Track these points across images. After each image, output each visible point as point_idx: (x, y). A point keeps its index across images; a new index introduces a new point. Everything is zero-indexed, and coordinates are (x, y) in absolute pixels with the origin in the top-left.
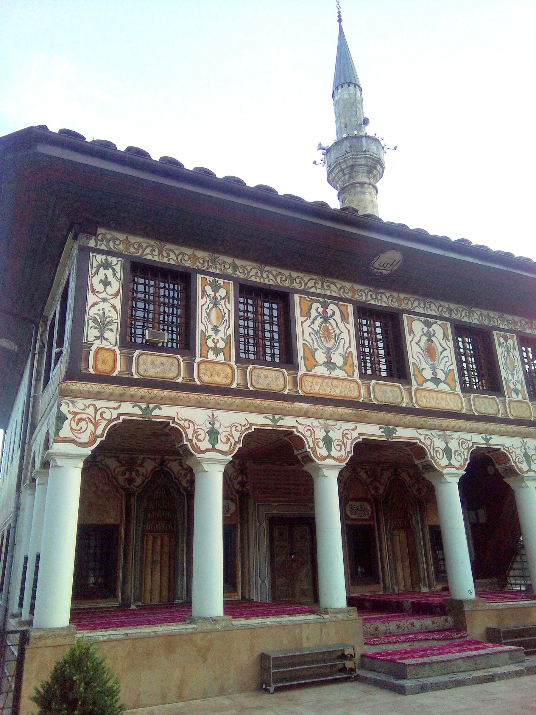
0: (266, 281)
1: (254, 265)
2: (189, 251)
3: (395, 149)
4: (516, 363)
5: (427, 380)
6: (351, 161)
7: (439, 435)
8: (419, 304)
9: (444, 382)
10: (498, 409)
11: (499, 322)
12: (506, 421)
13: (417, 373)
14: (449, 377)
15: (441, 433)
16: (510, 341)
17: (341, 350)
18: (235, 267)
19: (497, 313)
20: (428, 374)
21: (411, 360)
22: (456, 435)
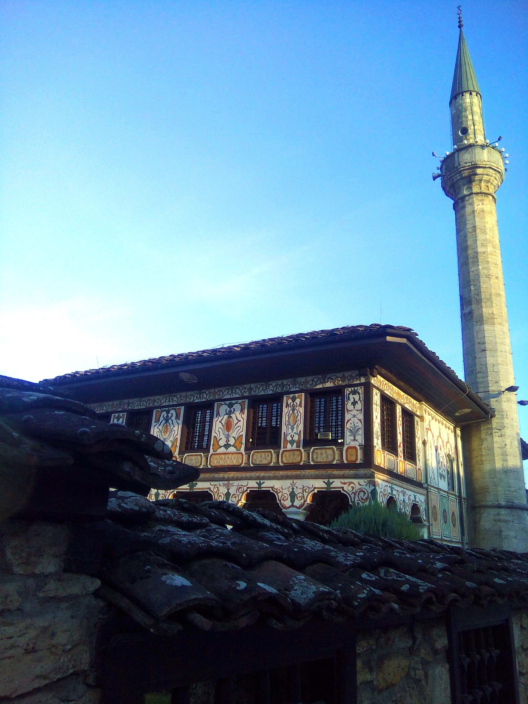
0: (141, 408)
1: (137, 399)
2: (110, 403)
3: (499, 139)
4: (299, 418)
5: (221, 447)
6: (449, 181)
7: (224, 485)
8: (228, 393)
9: (233, 446)
10: (272, 459)
11: (291, 386)
12: (277, 468)
13: (216, 443)
14: (238, 442)
15: (226, 482)
16: (298, 401)
17: (171, 439)
18: (129, 404)
19: (290, 380)
20: (222, 443)
21: (213, 434)
22: (236, 483)
